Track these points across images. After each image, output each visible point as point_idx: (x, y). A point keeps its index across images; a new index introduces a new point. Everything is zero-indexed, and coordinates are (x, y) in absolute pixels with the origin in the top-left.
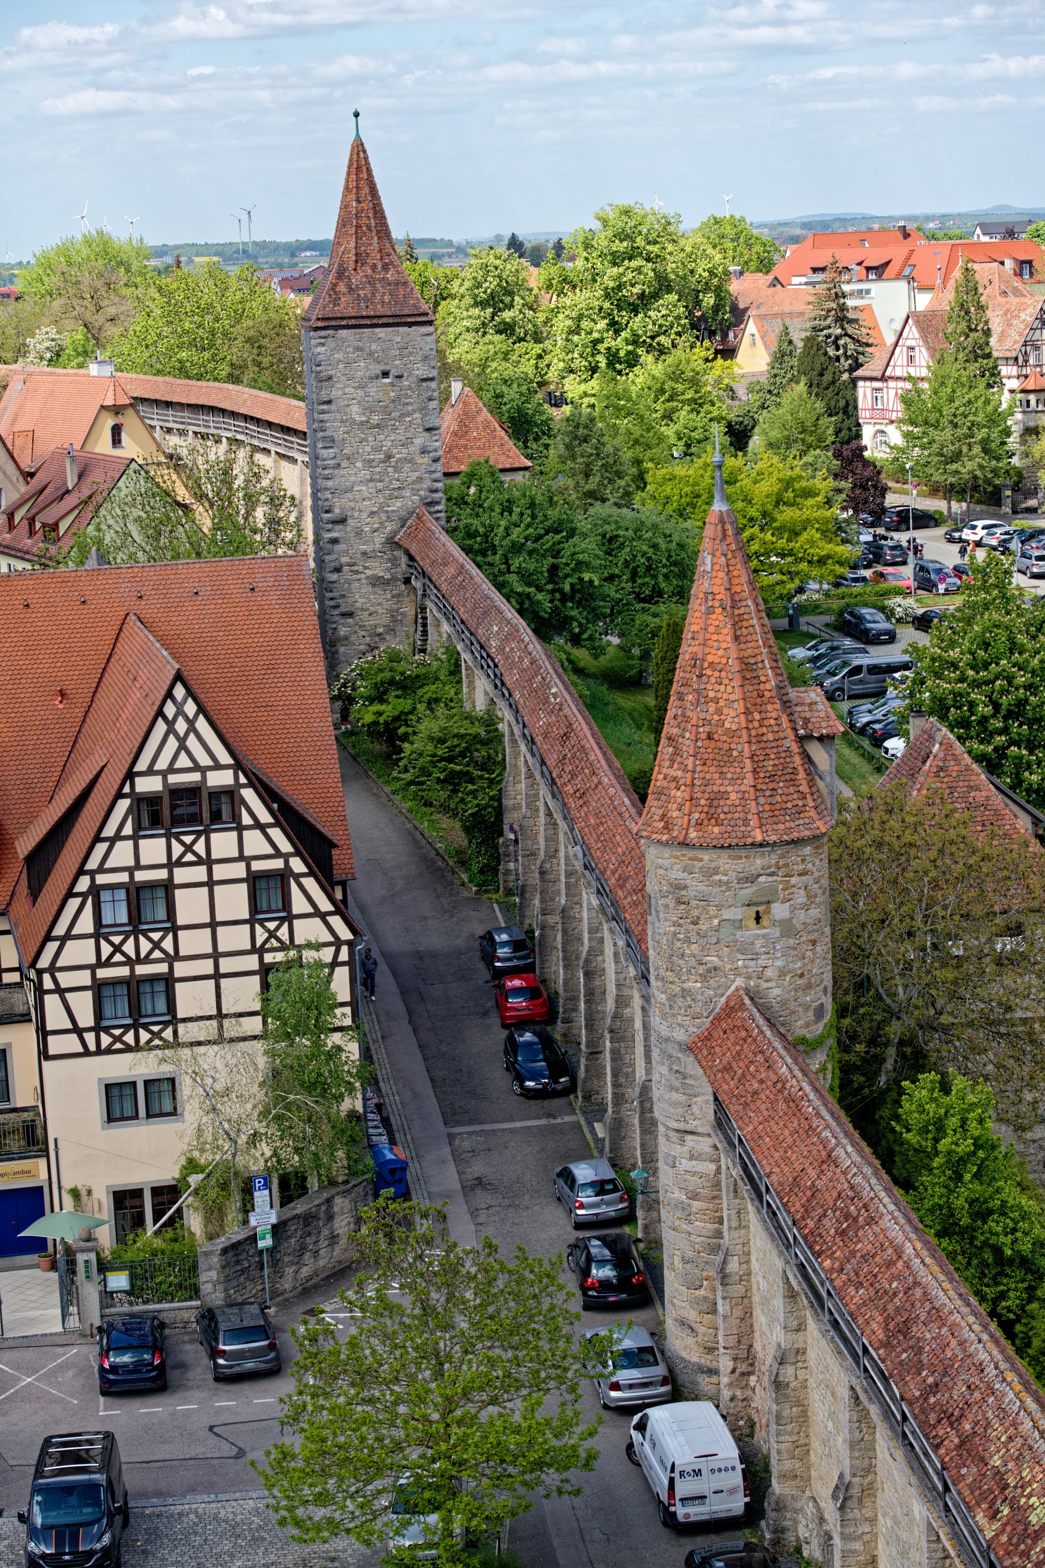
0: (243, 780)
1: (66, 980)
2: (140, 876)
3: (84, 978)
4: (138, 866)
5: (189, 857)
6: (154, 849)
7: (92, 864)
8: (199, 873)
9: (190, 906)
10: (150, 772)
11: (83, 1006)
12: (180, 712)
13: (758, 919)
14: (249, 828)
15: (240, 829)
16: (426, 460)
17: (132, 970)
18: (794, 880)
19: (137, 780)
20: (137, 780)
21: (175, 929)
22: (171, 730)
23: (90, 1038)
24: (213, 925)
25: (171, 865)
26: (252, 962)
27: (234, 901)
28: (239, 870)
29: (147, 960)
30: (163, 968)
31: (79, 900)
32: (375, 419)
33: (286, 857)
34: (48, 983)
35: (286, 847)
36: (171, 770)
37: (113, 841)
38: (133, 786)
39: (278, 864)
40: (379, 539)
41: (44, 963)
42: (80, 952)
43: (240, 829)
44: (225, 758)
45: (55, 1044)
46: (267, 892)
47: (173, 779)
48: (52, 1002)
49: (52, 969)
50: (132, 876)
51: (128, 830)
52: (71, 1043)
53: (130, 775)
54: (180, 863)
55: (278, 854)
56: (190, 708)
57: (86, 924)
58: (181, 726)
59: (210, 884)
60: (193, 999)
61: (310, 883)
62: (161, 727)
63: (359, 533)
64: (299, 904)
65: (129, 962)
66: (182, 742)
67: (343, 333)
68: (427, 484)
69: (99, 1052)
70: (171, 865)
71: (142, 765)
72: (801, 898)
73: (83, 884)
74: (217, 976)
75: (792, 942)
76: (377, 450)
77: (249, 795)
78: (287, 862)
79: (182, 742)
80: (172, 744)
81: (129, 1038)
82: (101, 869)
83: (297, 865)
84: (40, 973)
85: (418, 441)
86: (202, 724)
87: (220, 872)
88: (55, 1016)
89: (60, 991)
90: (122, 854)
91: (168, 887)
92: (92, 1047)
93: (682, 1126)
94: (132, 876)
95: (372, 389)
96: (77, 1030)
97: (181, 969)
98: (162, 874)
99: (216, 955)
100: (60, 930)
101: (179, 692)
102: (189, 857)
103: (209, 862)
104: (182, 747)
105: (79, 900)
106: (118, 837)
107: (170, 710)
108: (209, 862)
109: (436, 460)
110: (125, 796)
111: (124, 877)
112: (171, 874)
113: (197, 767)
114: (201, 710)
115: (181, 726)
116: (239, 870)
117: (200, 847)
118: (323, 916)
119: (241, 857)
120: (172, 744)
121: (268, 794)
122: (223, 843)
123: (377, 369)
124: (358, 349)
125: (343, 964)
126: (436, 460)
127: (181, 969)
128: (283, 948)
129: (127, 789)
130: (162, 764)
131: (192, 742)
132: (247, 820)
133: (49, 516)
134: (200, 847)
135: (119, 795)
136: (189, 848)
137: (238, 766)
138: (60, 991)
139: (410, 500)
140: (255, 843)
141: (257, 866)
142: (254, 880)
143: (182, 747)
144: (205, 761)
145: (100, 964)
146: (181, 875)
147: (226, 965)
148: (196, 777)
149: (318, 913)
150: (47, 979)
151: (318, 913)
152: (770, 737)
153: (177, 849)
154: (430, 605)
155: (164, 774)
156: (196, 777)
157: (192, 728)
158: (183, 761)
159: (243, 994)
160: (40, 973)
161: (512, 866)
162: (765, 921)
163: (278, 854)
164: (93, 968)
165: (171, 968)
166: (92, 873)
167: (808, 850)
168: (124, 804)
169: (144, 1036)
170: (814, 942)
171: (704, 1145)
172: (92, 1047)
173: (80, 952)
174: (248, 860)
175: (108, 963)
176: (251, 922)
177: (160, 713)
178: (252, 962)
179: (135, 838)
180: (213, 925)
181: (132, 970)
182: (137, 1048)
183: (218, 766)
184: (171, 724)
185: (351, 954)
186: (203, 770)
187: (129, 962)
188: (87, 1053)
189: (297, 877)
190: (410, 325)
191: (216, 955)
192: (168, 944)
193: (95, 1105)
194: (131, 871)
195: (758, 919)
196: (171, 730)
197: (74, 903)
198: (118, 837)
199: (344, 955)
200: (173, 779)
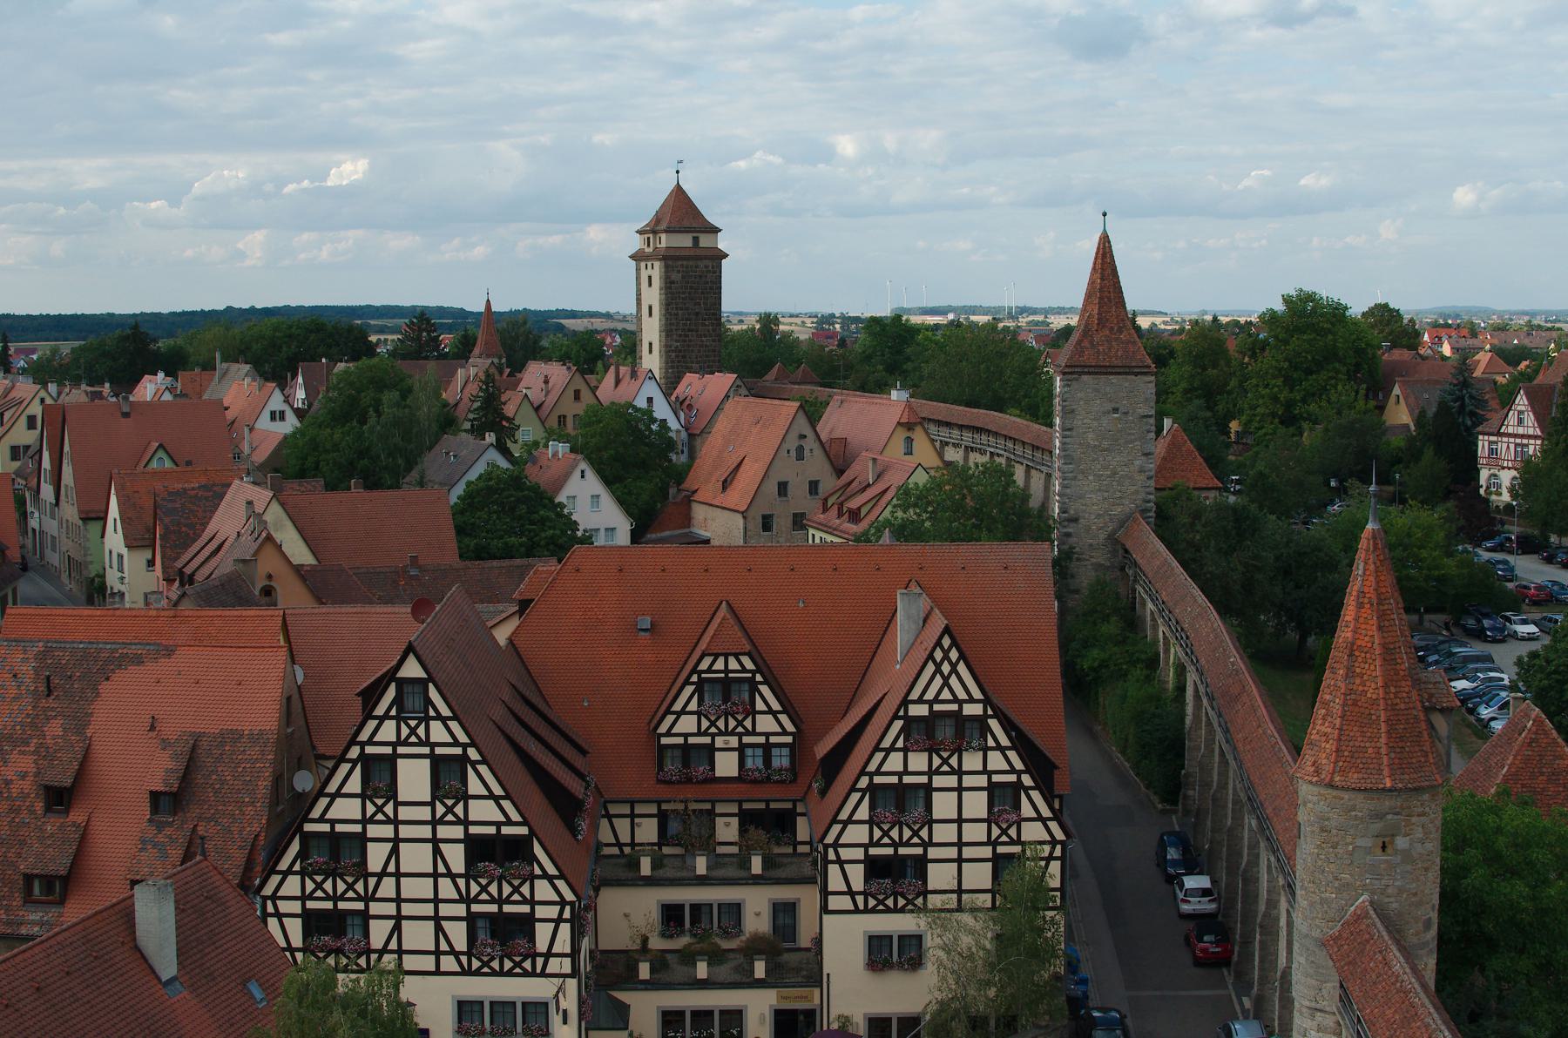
0: (990, 712)
1: (845, 854)
2: (907, 779)
3: (859, 854)
4: (906, 772)
5: (945, 768)
6: (918, 761)
7: (872, 767)
8: (952, 781)
9: (943, 805)
10: (920, 701)
11: (857, 875)
12: (946, 657)
13: (1384, 847)
14: (992, 749)
15: (985, 750)
16: (1143, 477)
17: (896, 851)
18: (1414, 819)
19: (911, 707)
20: (911, 707)
21: (930, 822)
22: (938, 670)
23: (860, 899)
24: (960, 821)
25: (931, 773)
26: (987, 852)
27: (977, 804)
28: (982, 781)
29: (908, 844)
30: (919, 851)
31: (859, 795)
32: (1105, 444)
33: (1019, 773)
34: (832, 856)
35: (1019, 765)
36: (936, 700)
37: (888, 751)
38: (906, 711)
39: (1013, 778)
40: (1102, 536)
41: (830, 839)
42: (858, 834)
43: (985, 750)
44: (977, 694)
45: (834, 902)
46: (1003, 798)
47: (937, 707)
48: (834, 870)
49: (836, 845)
50: (900, 779)
51: (900, 744)
52: (845, 902)
53: (905, 702)
54: (938, 772)
55: (1012, 770)
56: (954, 655)
57: (863, 813)
58: (946, 668)
59: (960, 789)
60: (940, 876)
61: (1035, 795)
62: (931, 668)
63: (1088, 529)
64: (1027, 810)
65: (895, 845)
66: (946, 680)
67: (1085, 378)
68: (1142, 496)
69: (866, 911)
70: (931, 773)
71: (915, 695)
72: (1419, 833)
73: (864, 782)
74: (960, 860)
75: (1409, 867)
76: (1105, 468)
77: (994, 724)
78: (1019, 778)
79: (946, 680)
80: (938, 681)
81: (890, 902)
82: (878, 772)
83: (1027, 780)
84: (826, 847)
85: (1137, 462)
86: (962, 668)
87: (968, 781)
88: (835, 881)
89: (840, 862)
90: (895, 762)
91: (928, 789)
92: (861, 907)
93: (1313, 1005)
94: (900, 779)
95: (1104, 421)
96: (851, 893)
97: (933, 853)
98: (924, 779)
99: (960, 844)
100: (844, 816)
101: (946, 642)
102: (945, 768)
103: (959, 772)
104: (946, 683)
105: (859, 795)
106: (892, 748)
107: (938, 655)
108: (959, 772)
109: (1149, 478)
110: (900, 718)
111: (895, 779)
112: (930, 779)
113: (955, 700)
114: (962, 656)
115: (946, 668)
116: (982, 781)
117: (954, 761)
118: (1044, 821)
119: (985, 771)
120: (938, 681)
121: (1008, 725)
122: (972, 761)
123: (1109, 406)
124: (1097, 390)
125: (1056, 859)
126: (1149, 478)
127: (933, 853)
128: (1012, 842)
129: (901, 713)
130: (930, 696)
131: (953, 681)
132: (991, 743)
133: (853, 504)
134: (954, 761)
135: (896, 717)
136: (945, 761)
137: (986, 702)
138: (840, 862)
139: (1129, 506)
140: (996, 761)
141: (995, 778)
142: (992, 788)
143: (946, 683)
144: (962, 695)
145: (872, 844)
146: (938, 781)
147: (968, 852)
148: (955, 707)
149: (1040, 818)
150: (831, 851)
151: (1040, 818)
152: (1403, 706)
153: (936, 761)
154: (1139, 588)
155: (931, 703)
156: (955, 707)
157: (954, 670)
158: (946, 695)
159: (979, 876)
160: (826, 847)
161: (1191, 793)
162: (1389, 850)
163: (1012, 770)
164: (866, 847)
165: (925, 851)
166: (871, 775)
167: (1426, 797)
168: (898, 724)
169: (901, 902)
170: (1426, 869)
171: (1329, 1021)
172: (861, 907)
173: (858, 834)
174: (990, 774)
175: (878, 844)
176: (988, 821)
177: (931, 657)
178: (987, 852)
179: (905, 750)
180: (960, 821)
181: (896, 851)
182: (896, 910)
183: (971, 700)
184: (938, 666)
185: (1063, 850)
186: (961, 703)
187: (895, 845)
188: (857, 911)
189: (1026, 789)
190: (1136, 374)
191: (960, 844)
192: (924, 833)
193: (858, 953)
194: (900, 775)
195: (1384, 847)
196: (938, 670)
197: (855, 796)
198: (892, 748)
199: (1058, 852)
200: (937, 707)
